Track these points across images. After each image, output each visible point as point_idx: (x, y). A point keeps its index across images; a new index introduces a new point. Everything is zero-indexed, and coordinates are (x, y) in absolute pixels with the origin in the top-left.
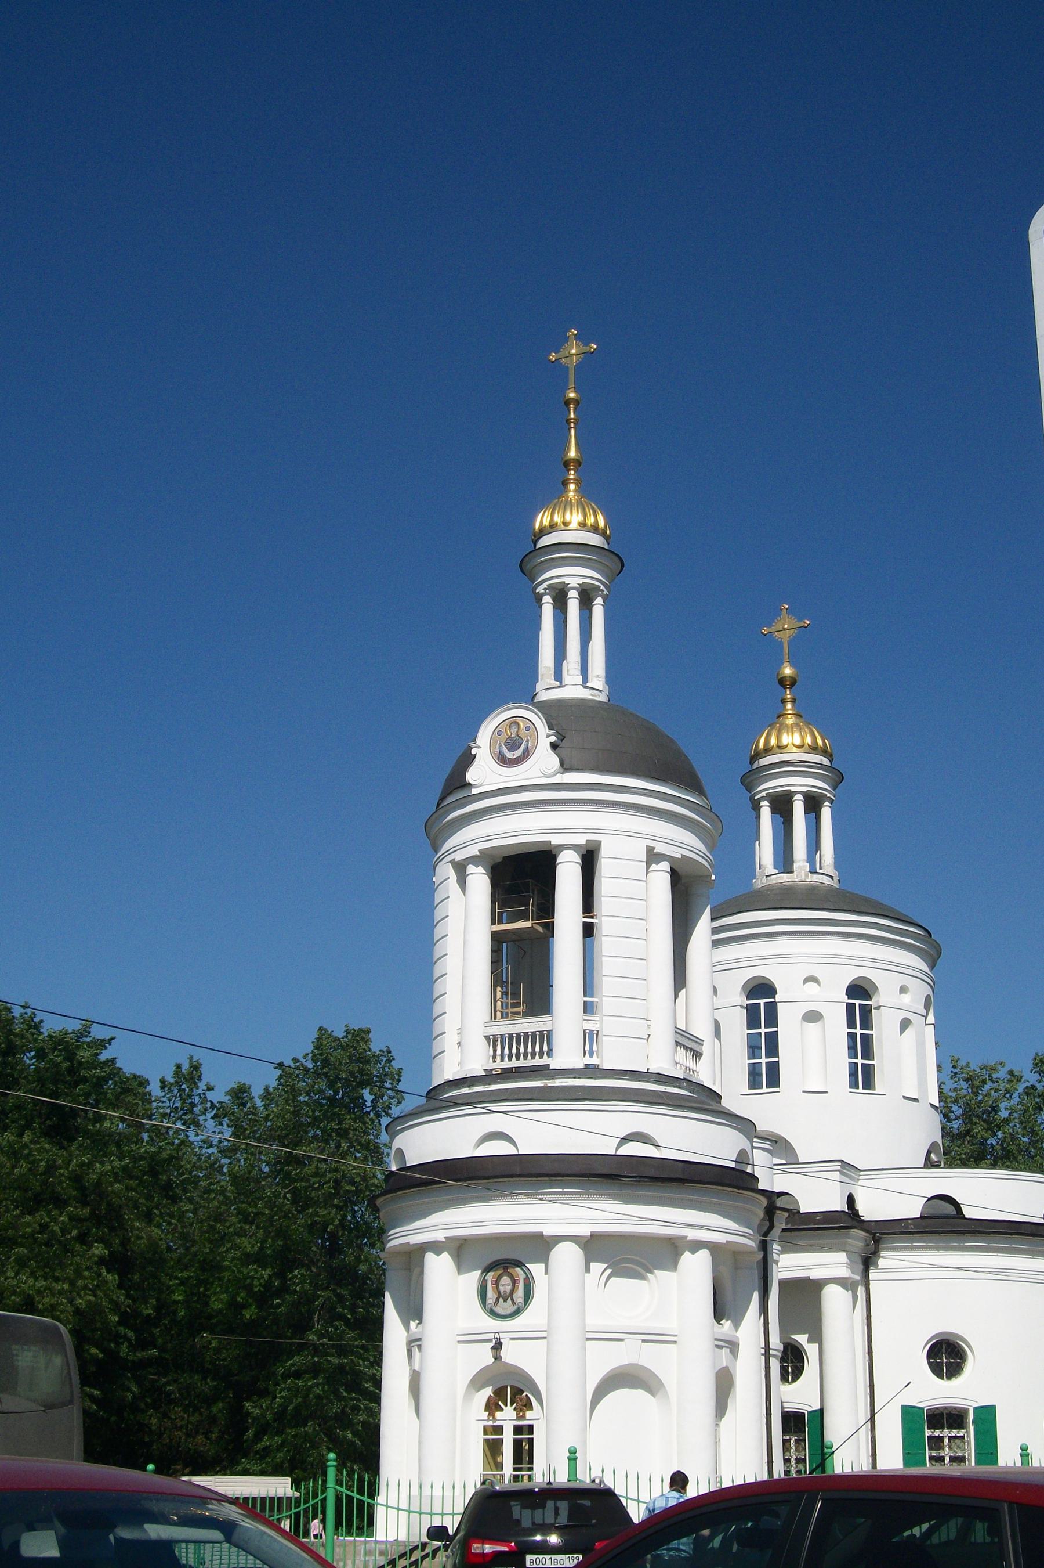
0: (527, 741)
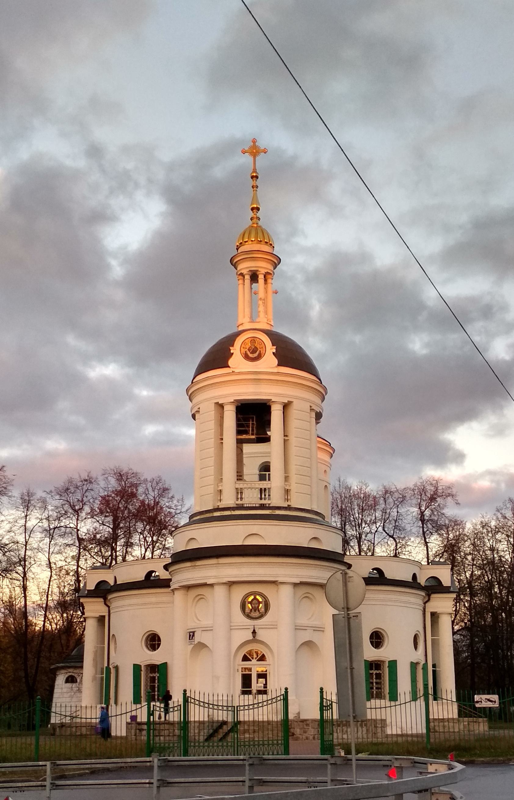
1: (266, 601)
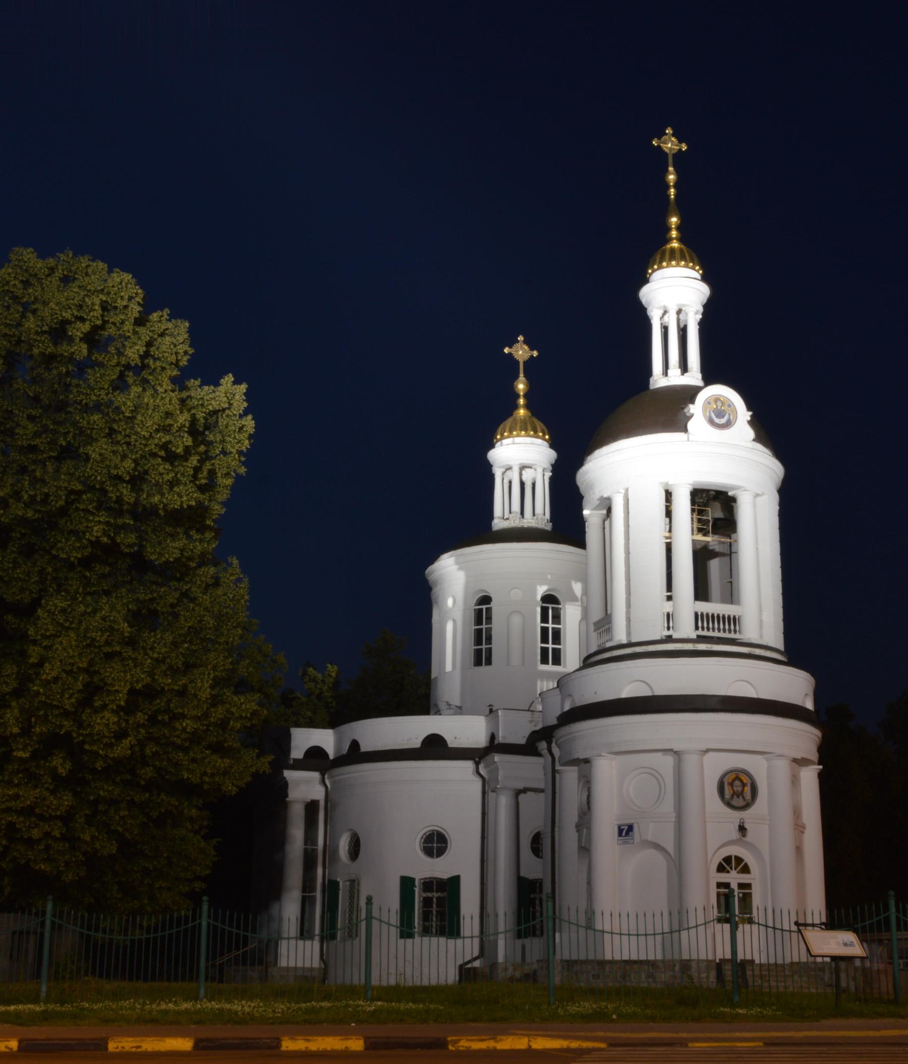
0: (729, 414)
1: (753, 782)
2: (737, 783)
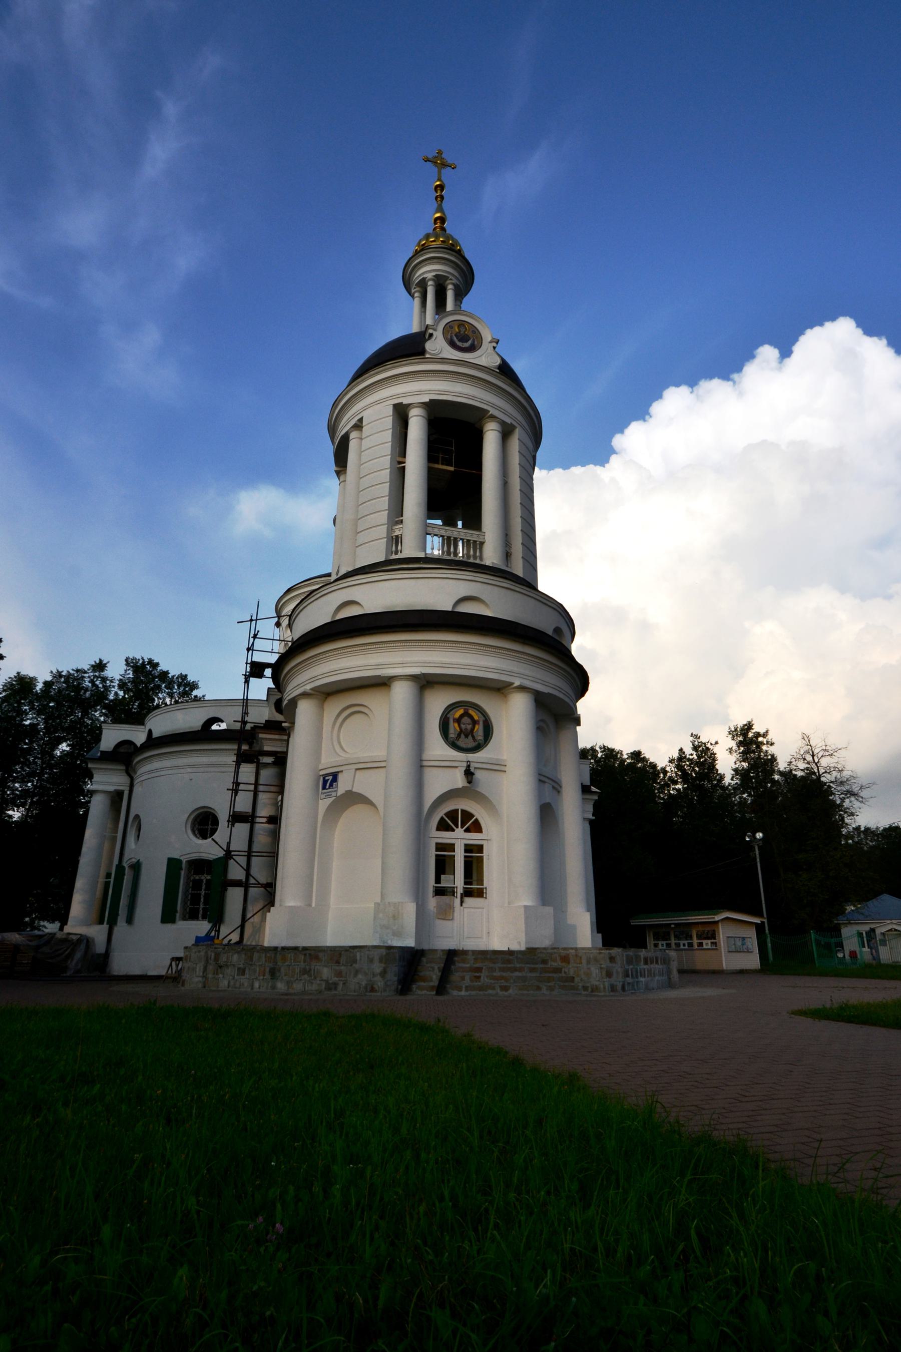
0: (474, 340)
1: (486, 720)
2: (466, 720)
